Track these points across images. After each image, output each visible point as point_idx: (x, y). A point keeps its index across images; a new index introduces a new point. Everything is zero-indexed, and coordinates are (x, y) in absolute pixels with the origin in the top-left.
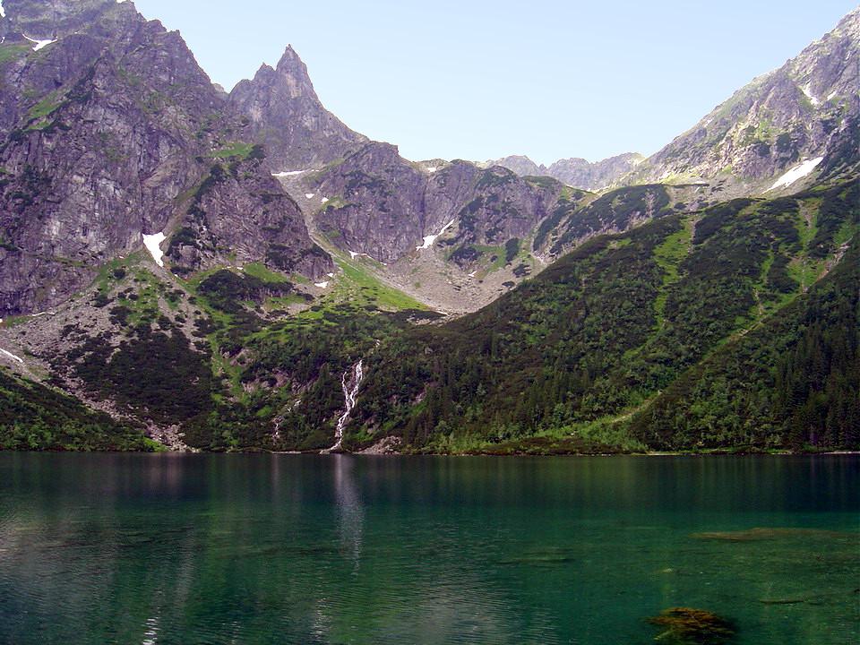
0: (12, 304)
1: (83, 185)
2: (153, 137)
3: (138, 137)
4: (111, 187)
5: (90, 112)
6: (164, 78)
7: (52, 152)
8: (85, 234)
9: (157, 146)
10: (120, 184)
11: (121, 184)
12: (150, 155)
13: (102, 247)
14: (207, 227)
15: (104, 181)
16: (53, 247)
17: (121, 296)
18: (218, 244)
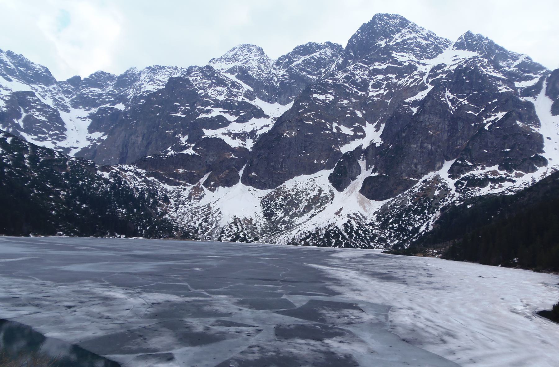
1: (416, 148)
3: (447, 123)
4: (430, 146)
5: (422, 118)
7: (405, 137)
8: (416, 167)
9: (457, 124)
10: (433, 144)
13: (424, 170)
14: (471, 156)
16: (402, 173)
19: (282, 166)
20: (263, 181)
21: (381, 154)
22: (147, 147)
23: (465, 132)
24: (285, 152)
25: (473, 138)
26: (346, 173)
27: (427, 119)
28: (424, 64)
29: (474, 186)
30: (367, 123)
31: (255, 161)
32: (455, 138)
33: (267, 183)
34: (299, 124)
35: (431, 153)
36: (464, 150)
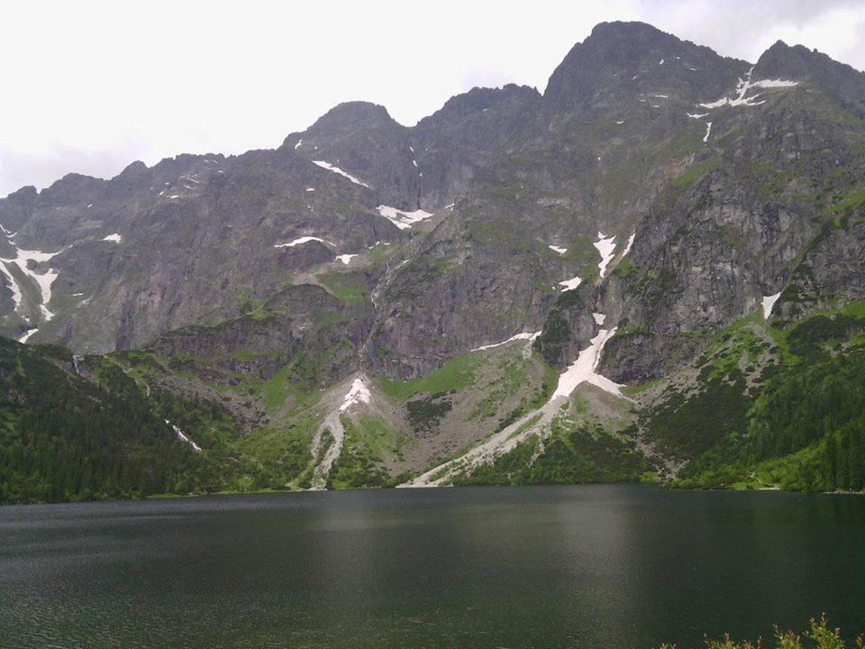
2: (771, 214)
3: (757, 218)
4: (728, 267)
6: (792, 156)
7: (677, 254)
10: (736, 263)
11: (737, 263)
12: (771, 229)
15: (721, 265)
16: (678, 325)
17: (716, 356)
18: (829, 290)
19: (441, 331)
20: (405, 361)
21: (633, 290)
22: (171, 312)
23: (798, 236)
24: (444, 302)
25: (814, 245)
27: (717, 215)
28: (703, 110)
29: (825, 338)
30: (601, 236)
31: (390, 322)
32: (776, 247)
33: (414, 364)
34: (468, 245)
35: (732, 280)
36: (796, 271)
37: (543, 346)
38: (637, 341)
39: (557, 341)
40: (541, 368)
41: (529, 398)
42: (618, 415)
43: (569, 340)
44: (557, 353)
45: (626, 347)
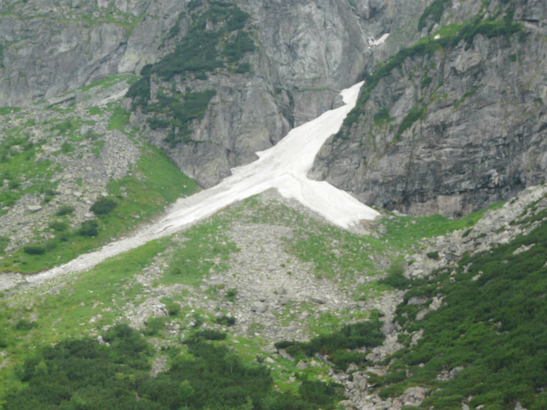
0: (501, 170)
26: (240, 49)
37: (154, 89)
38: (462, 60)
39: (200, 72)
40: (123, 155)
41: (25, 236)
42: (298, 283)
43: (245, 69)
44: (196, 107)
45: (427, 82)
